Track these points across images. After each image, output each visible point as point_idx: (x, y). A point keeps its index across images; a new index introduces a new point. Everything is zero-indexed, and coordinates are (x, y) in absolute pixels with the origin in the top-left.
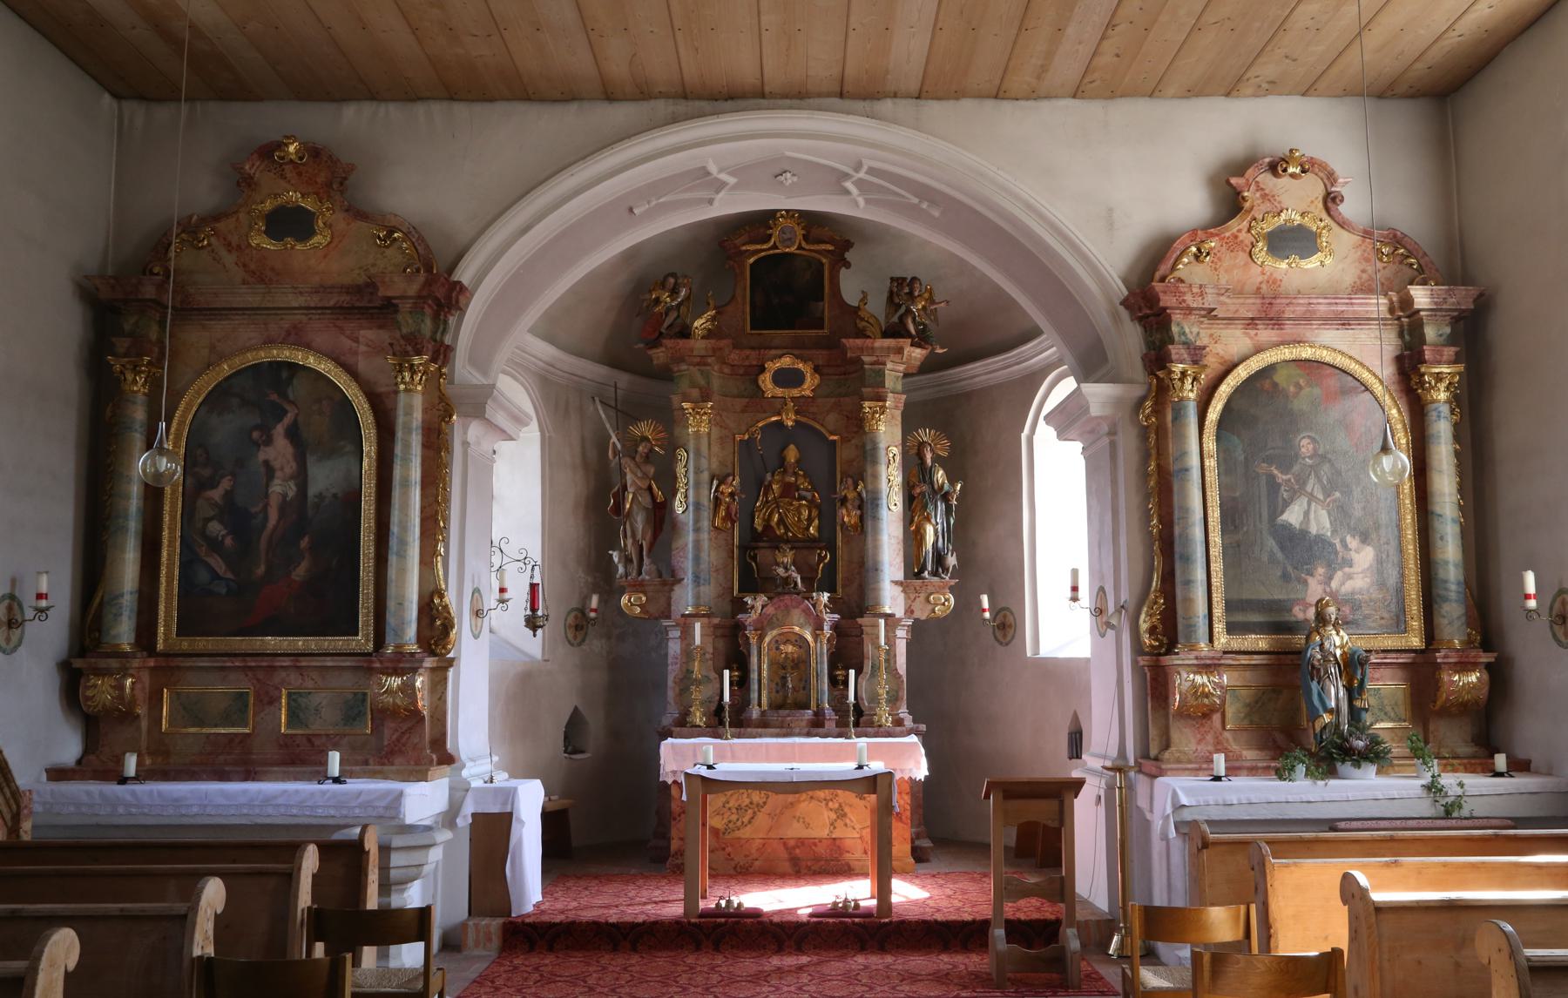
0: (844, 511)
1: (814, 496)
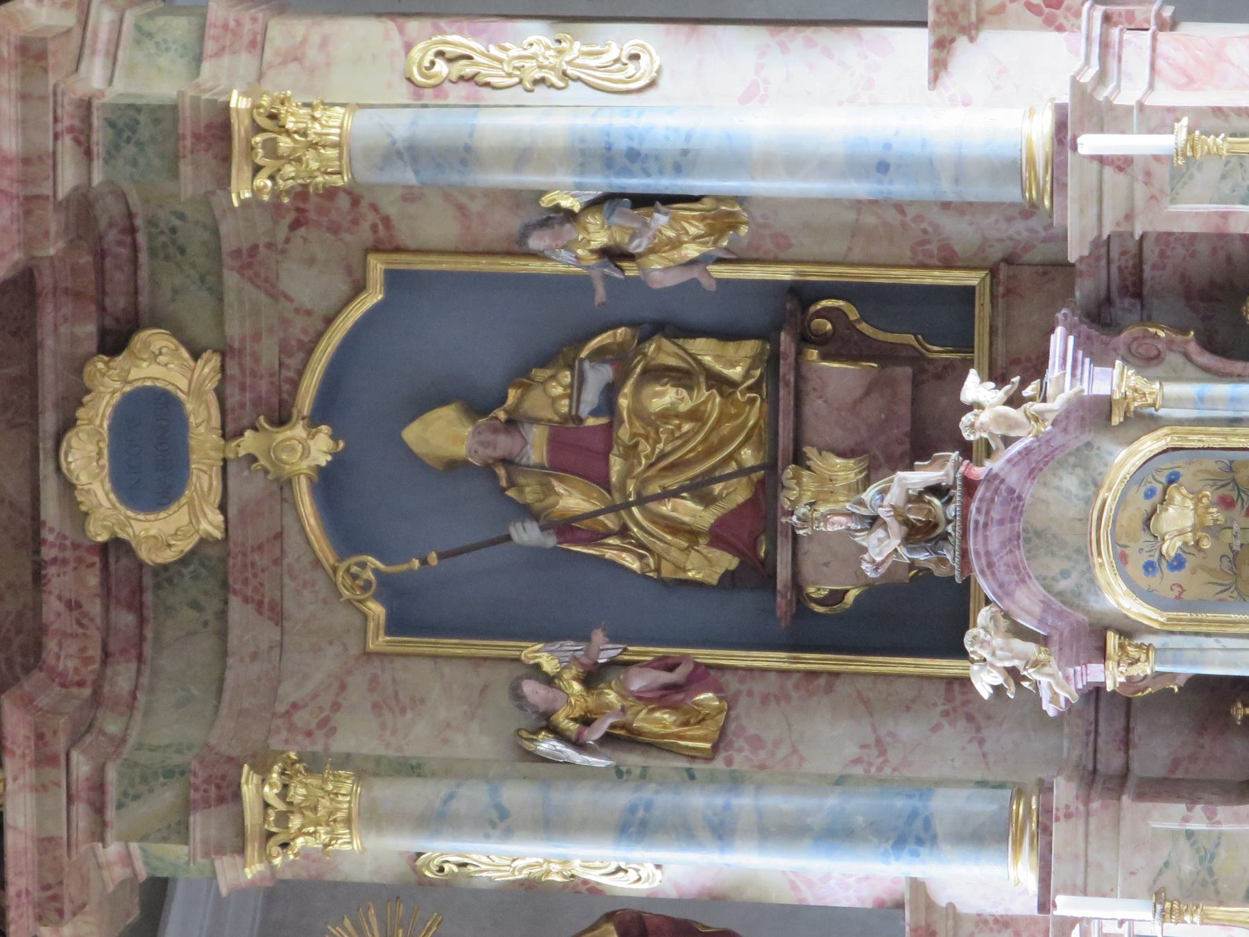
0: (656, 264)
1: (600, 355)
